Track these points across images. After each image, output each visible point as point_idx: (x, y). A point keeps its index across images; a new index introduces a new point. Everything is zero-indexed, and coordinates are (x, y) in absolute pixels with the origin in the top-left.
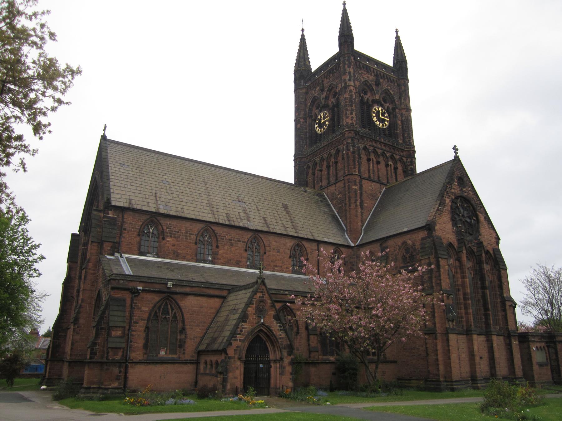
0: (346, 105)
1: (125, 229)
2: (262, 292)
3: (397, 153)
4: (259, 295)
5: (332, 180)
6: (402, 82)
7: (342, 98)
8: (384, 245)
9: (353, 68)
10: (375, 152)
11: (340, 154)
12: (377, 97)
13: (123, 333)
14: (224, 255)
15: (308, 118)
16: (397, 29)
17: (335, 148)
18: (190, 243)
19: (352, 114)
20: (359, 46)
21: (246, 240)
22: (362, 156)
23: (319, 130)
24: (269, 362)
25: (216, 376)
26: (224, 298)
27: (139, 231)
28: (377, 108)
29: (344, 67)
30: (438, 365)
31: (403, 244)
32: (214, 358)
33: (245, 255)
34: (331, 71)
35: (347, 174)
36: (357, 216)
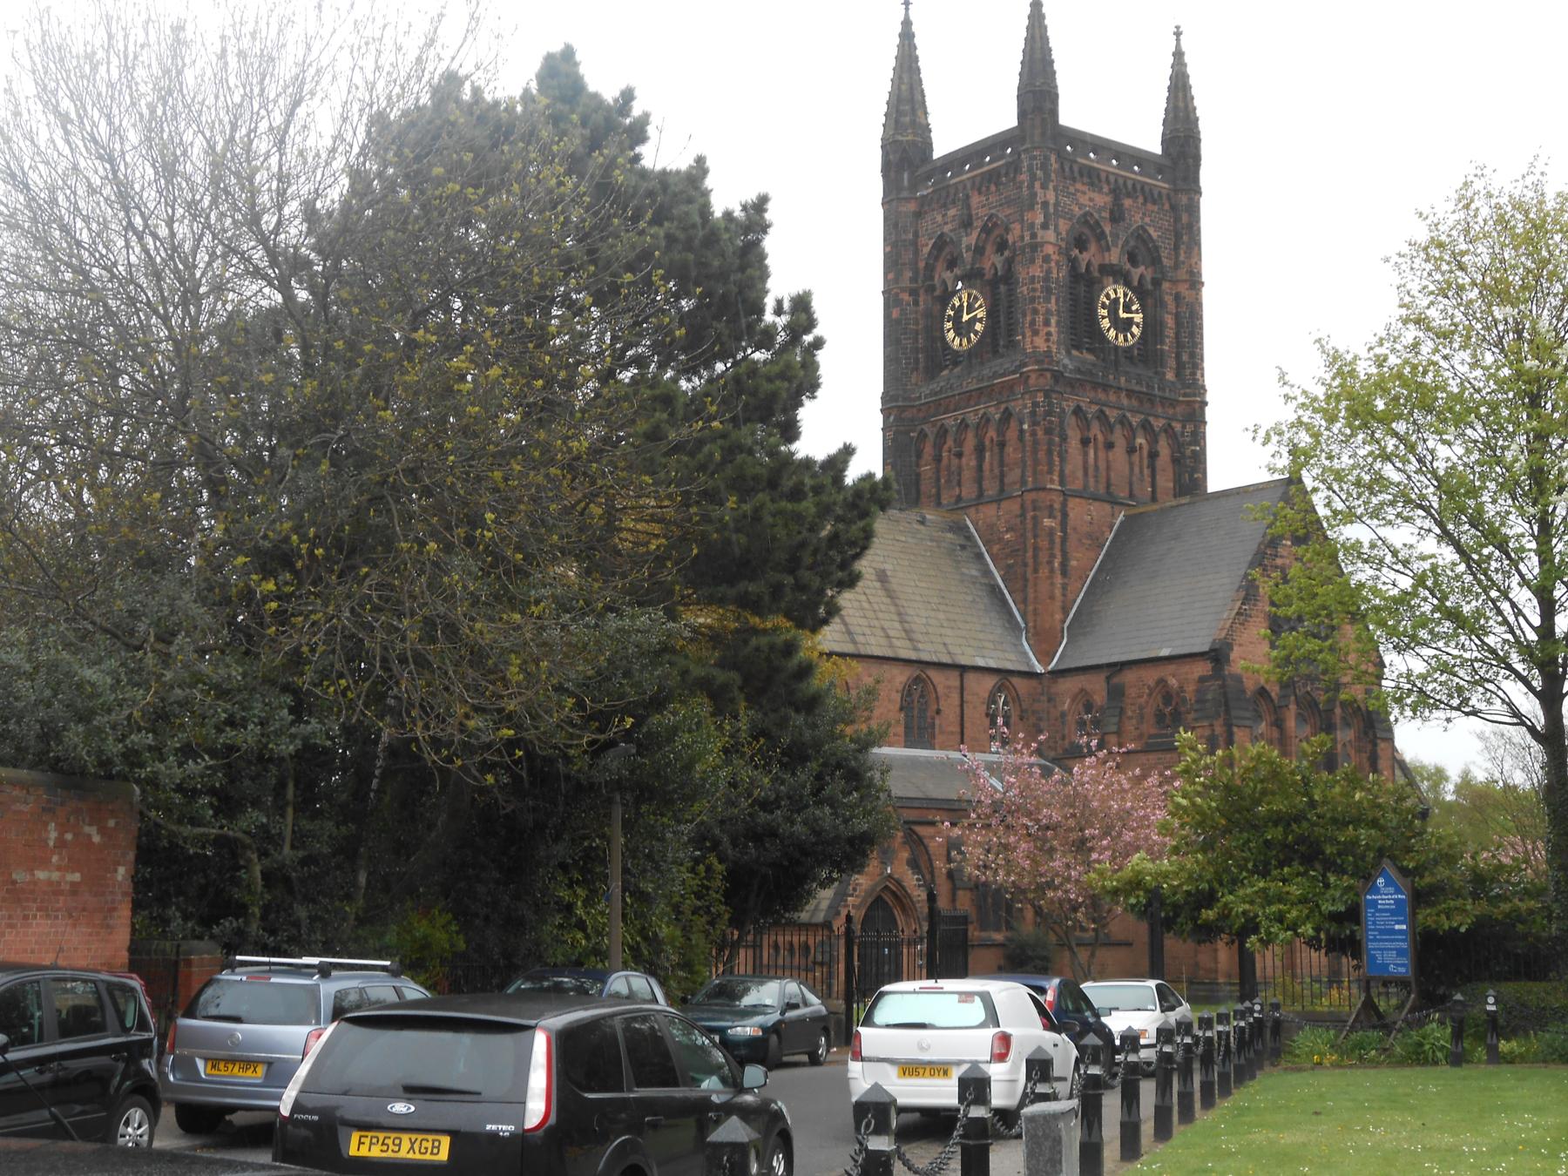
0: (1033, 300)
3: (1160, 410)
5: (991, 489)
8: (1115, 680)
9: (1055, 189)
10: (1101, 417)
11: (1013, 424)
12: (1114, 256)
15: (922, 292)
17: (1000, 403)
19: (1047, 323)
20: (1071, 115)
22: (1070, 433)
29: (1031, 186)
35: (1030, 486)
36: (1052, 597)
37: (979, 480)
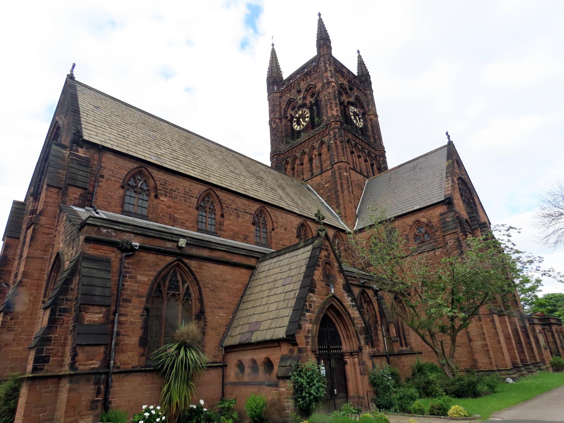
0: (330, 99)
1: (102, 177)
2: (327, 250)
4: (324, 253)
5: (316, 171)
6: (369, 92)
7: (321, 96)
13: (106, 317)
14: (230, 227)
16: (358, 50)
18: (190, 206)
21: (253, 212)
23: (296, 127)
24: (342, 355)
25: (276, 385)
26: (252, 268)
27: (123, 182)
28: (352, 108)
30: (488, 351)
31: (414, 223)
32: (260, 356)
33: (253, 228)
34: (309, 74)
37: (311, 170)
